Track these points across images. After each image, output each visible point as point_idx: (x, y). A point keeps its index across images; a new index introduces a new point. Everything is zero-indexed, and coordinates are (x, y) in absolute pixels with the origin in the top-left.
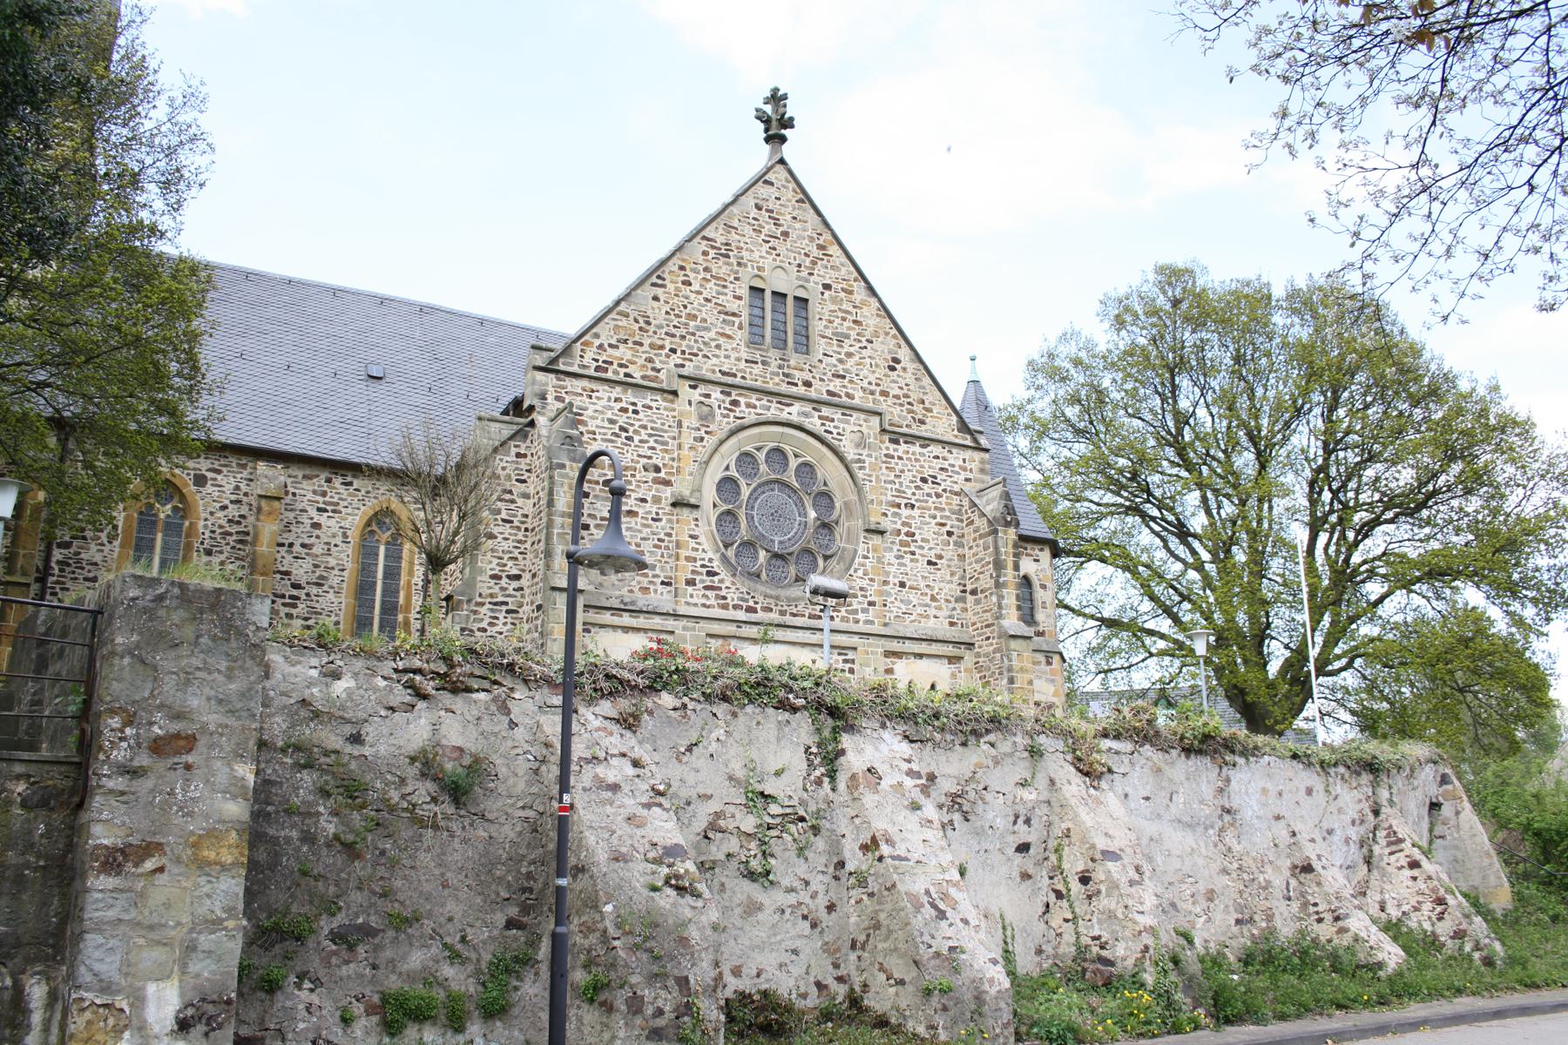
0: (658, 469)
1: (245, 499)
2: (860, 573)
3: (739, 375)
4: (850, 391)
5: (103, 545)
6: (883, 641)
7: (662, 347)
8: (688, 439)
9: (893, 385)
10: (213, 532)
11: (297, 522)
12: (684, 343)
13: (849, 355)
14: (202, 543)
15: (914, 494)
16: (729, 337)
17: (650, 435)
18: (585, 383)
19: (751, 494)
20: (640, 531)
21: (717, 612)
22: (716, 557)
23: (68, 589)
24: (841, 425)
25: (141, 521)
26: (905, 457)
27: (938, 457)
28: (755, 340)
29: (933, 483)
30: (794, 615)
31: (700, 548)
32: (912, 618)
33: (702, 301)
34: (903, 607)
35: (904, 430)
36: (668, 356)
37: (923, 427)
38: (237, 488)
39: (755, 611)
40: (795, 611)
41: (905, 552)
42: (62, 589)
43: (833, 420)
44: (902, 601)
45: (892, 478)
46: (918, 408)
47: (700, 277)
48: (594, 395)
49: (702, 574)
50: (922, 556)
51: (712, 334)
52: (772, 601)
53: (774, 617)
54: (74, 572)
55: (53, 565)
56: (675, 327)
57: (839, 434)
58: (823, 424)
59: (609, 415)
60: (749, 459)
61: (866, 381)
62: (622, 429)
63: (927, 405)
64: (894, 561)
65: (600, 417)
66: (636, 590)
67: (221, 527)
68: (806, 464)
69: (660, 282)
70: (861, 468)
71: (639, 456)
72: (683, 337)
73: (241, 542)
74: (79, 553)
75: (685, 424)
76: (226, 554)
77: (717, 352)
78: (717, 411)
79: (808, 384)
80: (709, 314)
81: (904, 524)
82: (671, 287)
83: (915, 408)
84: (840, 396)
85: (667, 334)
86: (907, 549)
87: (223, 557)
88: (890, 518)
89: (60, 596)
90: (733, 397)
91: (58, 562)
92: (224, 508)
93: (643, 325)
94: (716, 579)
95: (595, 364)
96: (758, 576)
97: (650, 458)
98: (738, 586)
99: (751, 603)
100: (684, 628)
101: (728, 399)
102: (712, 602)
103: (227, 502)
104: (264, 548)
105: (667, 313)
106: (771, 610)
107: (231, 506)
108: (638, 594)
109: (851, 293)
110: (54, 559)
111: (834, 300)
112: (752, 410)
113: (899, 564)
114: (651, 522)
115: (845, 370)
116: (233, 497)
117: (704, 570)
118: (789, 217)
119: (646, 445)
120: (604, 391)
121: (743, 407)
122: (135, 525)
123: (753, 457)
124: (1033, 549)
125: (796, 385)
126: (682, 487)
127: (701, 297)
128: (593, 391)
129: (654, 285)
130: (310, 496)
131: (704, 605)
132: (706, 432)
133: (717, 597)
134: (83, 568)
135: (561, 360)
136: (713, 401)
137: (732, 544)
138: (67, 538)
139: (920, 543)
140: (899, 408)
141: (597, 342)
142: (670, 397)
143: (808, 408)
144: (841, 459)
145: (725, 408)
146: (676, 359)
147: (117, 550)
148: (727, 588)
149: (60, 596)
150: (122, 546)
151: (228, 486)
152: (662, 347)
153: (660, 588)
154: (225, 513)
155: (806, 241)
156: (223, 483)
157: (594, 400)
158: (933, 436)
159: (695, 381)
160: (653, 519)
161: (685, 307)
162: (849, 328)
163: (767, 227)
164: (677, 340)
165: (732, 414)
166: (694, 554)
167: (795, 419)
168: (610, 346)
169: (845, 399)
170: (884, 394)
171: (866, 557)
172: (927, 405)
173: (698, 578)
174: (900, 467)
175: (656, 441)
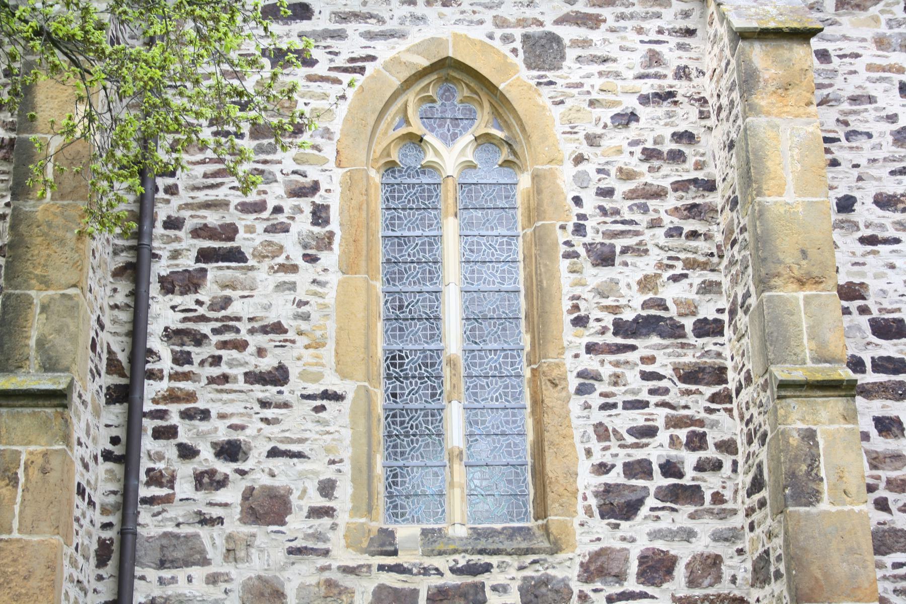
1: (682, 88)
5: (294, 269)
10: (608, 193)
11: (849, 135)
14: (579, 230)
23: (205, 415)
25: (392, 191)
38: (654, 59)
42: (187, 415)
54: (216, 361)
55: (155, 343)
67: (626, 175)
73: (693, 211)
74: (227, 302)
76: (656, 257)
87: (646, 265)
89: (183, 437)
91: (170, 335)
92: (628, 118)
103: (631, 103)
104: (790, 197)
107: (644, 112)
110: (155, 328)
116: (647, 87)
122: (378, 203)
130: (870, 54)
134: (241, 346)
138: (188, 262)
147: (334, 278)
149: (183, 437)
150: (347, 267)
151: (623, 57)
154: (633, 131)
156: (614, 52)
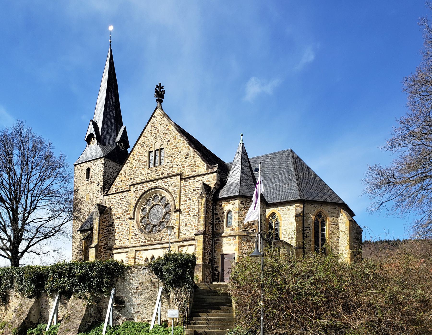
0: (127, 211)
3: (146, 178)
4: (174, 171)
6: (178, 243)
7: (129, 179)
8: (132, 201)
9: (186, 163)
12: (133, 176)
13: (174, 159)
15: (191, 195)
16: (143, 169)
17: (126, 203)
18: (113, 195)
20: (123, 228)
21: (138, 244)
22: (137, 230)
26: (189, 185)
27: (199, 181)
28: (149, 167)
29: (197, 190)
30: (155, 241)
31: (134, 229)
32: (188, 234)
33: (138, 162)
34: (186, 231)
35: (189, 176)
36: (130, 181)
37: (195, 173)
40: (155, 240)
41: (187, 214)
43: (167, 182)
44: (185, 230)
45: (185, 193)
46: (194, 167)
47: (137, 155)
48: (115, 198)
49: (134, 235)
50: (192, 214)
51: (140, 170)
52: (150, 238)
53: (150, 242)
56: (131, 172)
57: (169, 185)
58: (165, 184)
59: (118, 202)
61: (178, 165)
62: (121, 204)
63: (197, 165)
64: (184, 218)
65: (116, 202)
66: (122, 243)
68: (164, 197)
69: (128, 162)
71: (124, 209)
72: (133, 174)
75: (132, 198)
77: (141, 174)
78: (139, 191)
79: (162, 174)
80: (139, 165)
81: (188, 206)
82: (130, 161)
83: (193, 168)
84: (171, 173)
86: (188, 213)
88: (183, 205)
90: (143, 186)
93: (125, 175)
94: (137, 236)
95: (115, 190)
96: (151, 232)
97: (126, 209)
99: (145, 240)
100: (130, 250)
101: (142, 187)
102: (137, 242)
105: (130, 169)
106: (149, 241)
108: (123, 244)
109: (176, 139)
111: (170, 144)
112: (147, 187)
113: (185, 219)
114: (126, 225)
115: (173, 165)
117: (135, 234)
118: (159, 125)
119: (125, 206)
120: (117, 195)
121: (145, 188)
124: (233, 200)
125: (159, 175)
126: (131, 215)
127: (137, 161)
128: (115, 197)
129: (127, 163)
131: (135, 243)
132: (137, 198)
133: (138, 240)
135: (109, 192)
136: (138, 189)
139: (192, 210)
140: (188, 170)
141: (115, 184)
143: (161, 181)
144: (169, 192)
146: (132, 181)
148: (140, 237)
152: (129, 179)
153: (127, 241)
155: (164, 130)
157: (115, 199)
158: (197, 174)
159: (134, 185)
160: (126, 224)
161: (134, 166)
162: (174, 151)
163: (153, 131)
164: (132, 175)
165: (142, 190)
166: (132, 231)
167: (157, 185)
168: (118, 184)
169: (172, 173)
170: (184, 167)
171: (174, 219)
172: (197, 165)
173: (133, 236)
174: (187, 188)
175: (127, 204)
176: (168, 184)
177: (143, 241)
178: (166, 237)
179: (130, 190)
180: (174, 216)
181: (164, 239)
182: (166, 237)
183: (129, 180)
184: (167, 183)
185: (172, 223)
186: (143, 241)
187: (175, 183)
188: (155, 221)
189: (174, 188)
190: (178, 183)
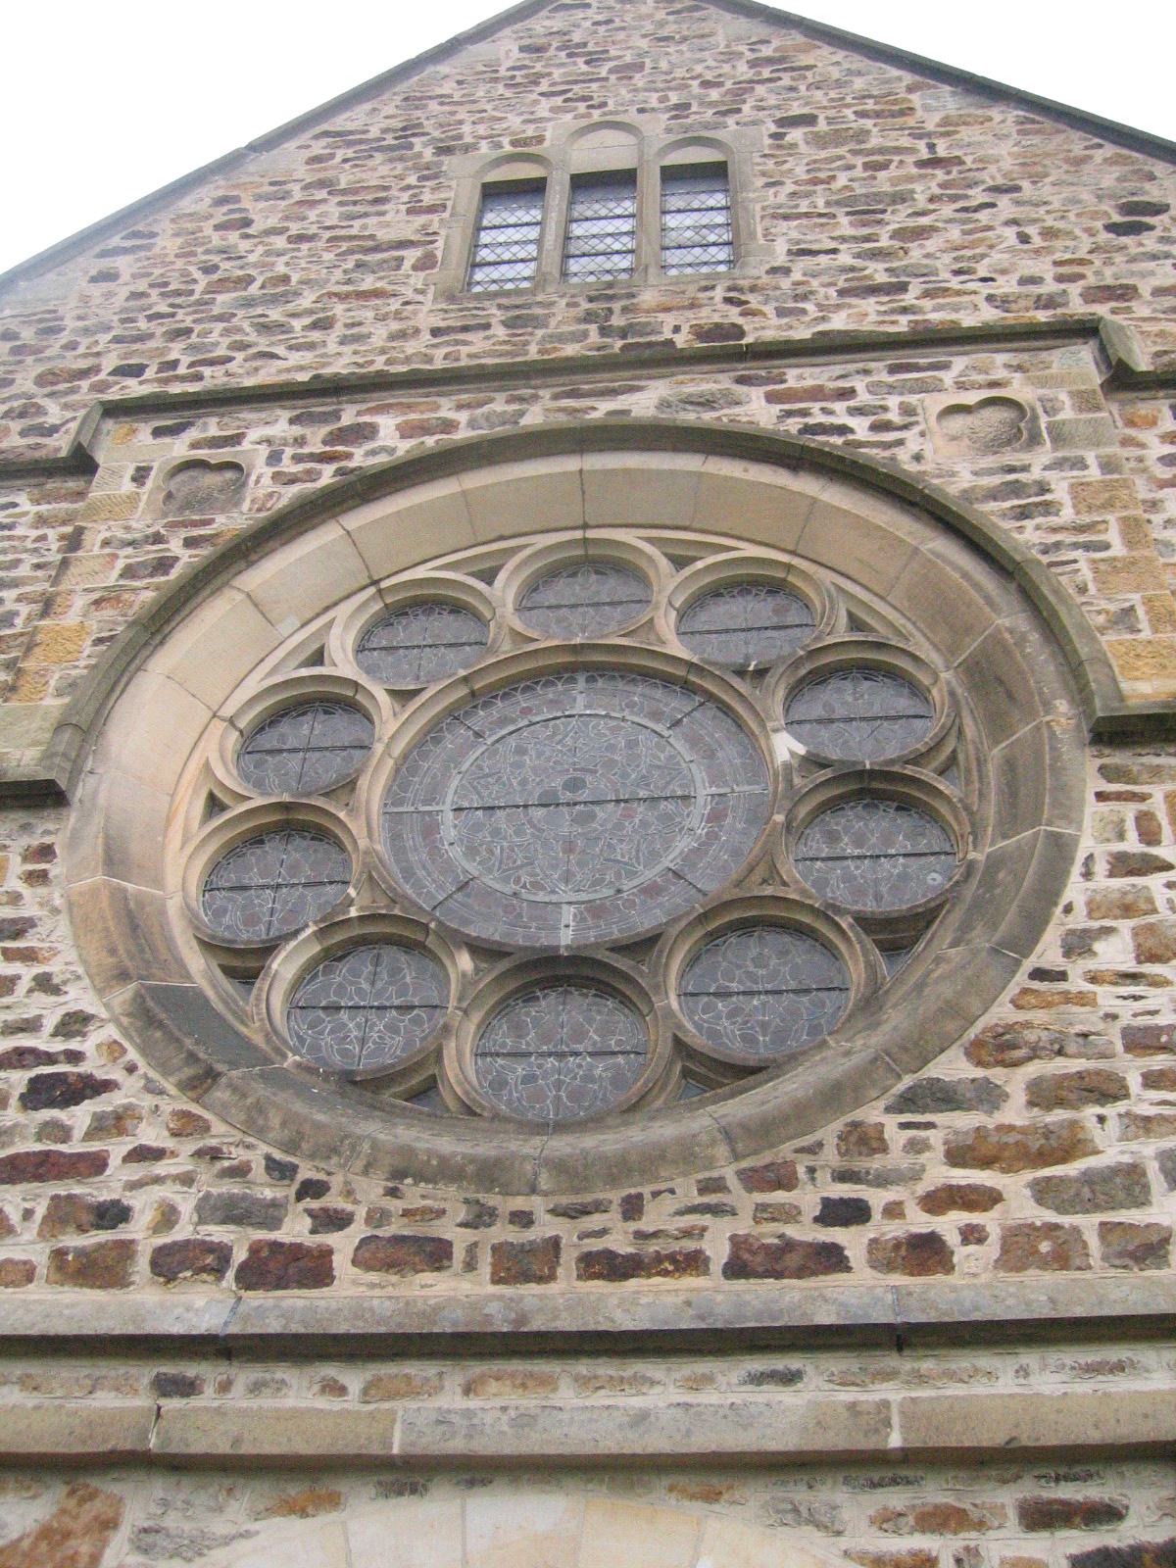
2: (1115, 952)
19: (432, 734)
24: (893, 401)
31: (27, 973)
39: (313, 1268)
40: (620, 1242)
60: (444, 626)
70: (1023, 513)
75: (93, 540)
78: (269, 471)
85: (117, 340)
94: (80, 1116)
96: (426, 1091)
98: (220, 1132)
99: (296, 1229)
106: (436, 1254)
123: (457, 608)
132: (189, 543)
133: (62, 1214)
137: (268, 950)
142: (72, 484)
145: (298, 459)
148: (142, 1154)
176: (867, 421)
177: (218, 1233)
178: (987, 1199)
179: (81, 463)
180: (1129, 811)
181: (926, 1253)
182: (987, 1199)
183: (102, 376)
184: (840, 407)
185: (1079, 920)
186: (218, 1233)
187: (996, 416)
188: (546, 911)
189: (1010, 458)
190: (1067, 413)
